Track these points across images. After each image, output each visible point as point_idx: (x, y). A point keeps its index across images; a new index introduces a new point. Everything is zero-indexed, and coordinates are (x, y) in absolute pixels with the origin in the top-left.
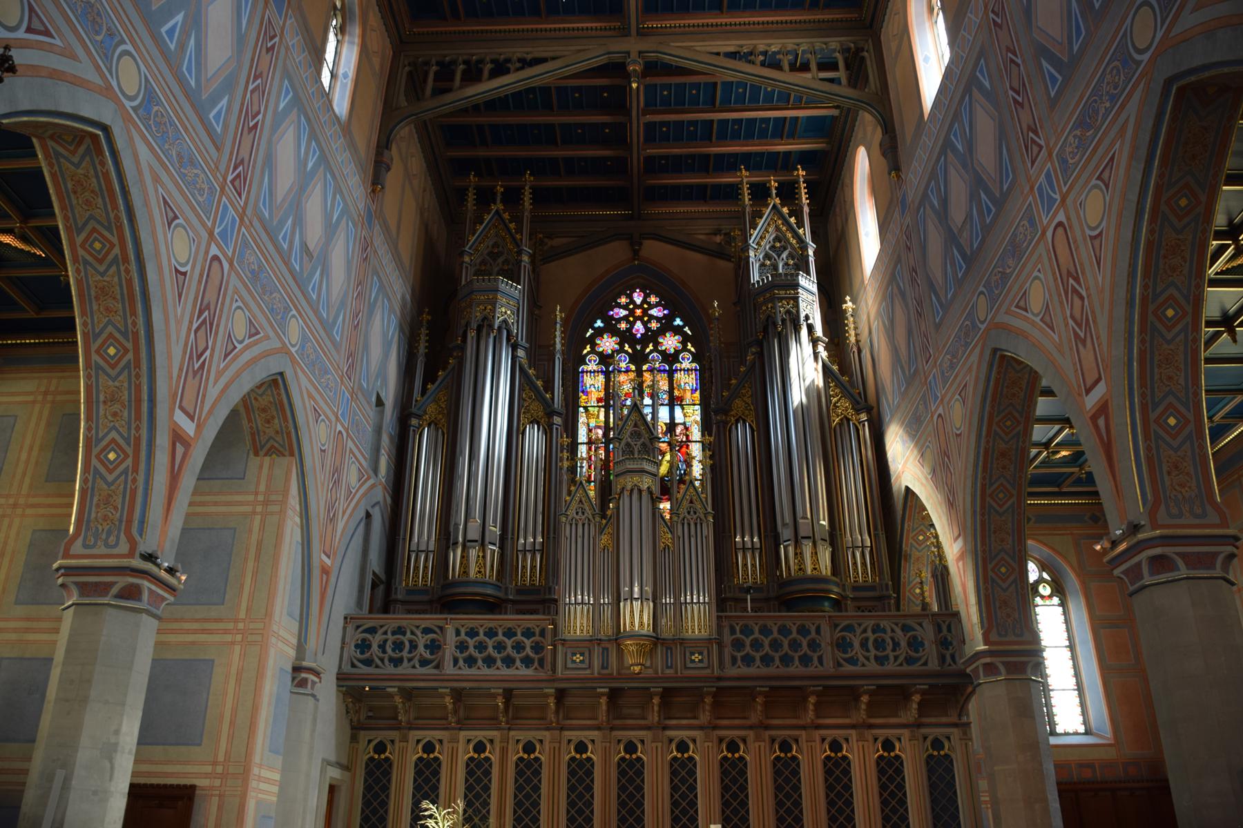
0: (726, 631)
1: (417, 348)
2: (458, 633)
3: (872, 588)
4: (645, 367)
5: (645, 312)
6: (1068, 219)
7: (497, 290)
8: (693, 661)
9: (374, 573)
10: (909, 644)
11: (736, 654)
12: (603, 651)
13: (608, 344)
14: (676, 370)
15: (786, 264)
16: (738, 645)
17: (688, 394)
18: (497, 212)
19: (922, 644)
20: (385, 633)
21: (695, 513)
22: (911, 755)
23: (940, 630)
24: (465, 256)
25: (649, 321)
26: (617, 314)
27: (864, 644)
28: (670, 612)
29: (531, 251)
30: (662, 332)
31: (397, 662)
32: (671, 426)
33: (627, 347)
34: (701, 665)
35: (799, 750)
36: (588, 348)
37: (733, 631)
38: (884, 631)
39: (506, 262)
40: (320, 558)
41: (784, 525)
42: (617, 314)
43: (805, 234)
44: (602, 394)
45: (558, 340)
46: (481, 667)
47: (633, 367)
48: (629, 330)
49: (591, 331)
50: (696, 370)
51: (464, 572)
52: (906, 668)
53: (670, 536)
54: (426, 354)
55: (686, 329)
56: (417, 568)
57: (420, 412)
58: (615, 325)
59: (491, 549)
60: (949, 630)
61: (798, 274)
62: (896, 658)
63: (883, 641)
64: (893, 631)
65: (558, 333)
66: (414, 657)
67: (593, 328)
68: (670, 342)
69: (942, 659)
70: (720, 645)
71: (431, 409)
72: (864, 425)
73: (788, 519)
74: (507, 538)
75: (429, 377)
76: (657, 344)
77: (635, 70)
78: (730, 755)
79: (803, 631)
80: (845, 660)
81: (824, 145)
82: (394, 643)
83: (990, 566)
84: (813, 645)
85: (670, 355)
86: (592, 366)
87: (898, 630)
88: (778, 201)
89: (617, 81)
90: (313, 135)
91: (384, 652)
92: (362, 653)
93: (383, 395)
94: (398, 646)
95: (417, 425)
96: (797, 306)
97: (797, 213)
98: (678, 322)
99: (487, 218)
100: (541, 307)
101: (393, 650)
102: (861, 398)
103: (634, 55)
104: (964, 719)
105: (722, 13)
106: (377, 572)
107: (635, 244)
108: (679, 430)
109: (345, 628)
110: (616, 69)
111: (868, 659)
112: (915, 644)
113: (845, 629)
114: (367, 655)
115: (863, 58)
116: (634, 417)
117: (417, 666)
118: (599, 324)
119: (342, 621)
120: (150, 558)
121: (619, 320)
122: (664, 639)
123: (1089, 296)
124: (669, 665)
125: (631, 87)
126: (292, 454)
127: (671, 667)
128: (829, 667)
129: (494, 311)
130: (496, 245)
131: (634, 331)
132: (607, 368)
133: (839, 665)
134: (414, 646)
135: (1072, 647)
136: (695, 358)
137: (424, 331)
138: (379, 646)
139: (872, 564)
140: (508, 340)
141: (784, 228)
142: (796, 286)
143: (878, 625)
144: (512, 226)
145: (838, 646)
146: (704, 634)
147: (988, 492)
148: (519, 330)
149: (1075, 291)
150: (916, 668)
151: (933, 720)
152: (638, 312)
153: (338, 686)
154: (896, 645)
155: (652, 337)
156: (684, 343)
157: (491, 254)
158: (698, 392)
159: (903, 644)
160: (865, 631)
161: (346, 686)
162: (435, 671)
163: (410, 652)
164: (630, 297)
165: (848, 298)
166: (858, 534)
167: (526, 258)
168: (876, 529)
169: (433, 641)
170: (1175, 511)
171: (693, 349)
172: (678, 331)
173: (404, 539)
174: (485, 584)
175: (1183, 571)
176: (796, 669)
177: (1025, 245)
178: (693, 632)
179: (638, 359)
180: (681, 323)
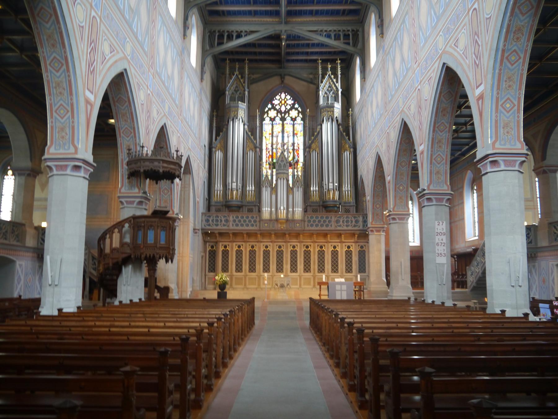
0: (306, 218)
2: (233, 217)
3: (350, 203)
6: (479, 7)
7: (238, 107)
13: (273, 113)
16: (309, 221)
17: (299, 132)
19: (359, 222)
22: (355, 250)
27: (343, 221)
28: (291, 213)
30: (291, 109)
31: (217, 225)
32: (293, 144)
33: (279, 115)
36: (266, 115)
37: (308, 217)
39: (240, 93)
40: (197, 199)
41: (325, 184)
44: (271, 132)
47: (281, 122)
48: (280, 109)
49: (267, 109)
56: (217, 195)
61: (334, 103)
62: (351, 225)
65: (258, 120)
68: (294, 113)
69: (364, 226)
71: (218, 146)
73: (327, 183)
75: (217, 135)
76: (289, 114)
77: (283, 38)
78: (306, 249)
80: (338, 226)
83: (374, 205)
84: (330, 221)
87: (353, 218)
88: (330, 73)
89: (277, 42)
90: (191, 81)
92: (207, 222)
94: (217, 221)
96: (333, 114)
97: (336, 77)
98: (296, 106)
99: (234, 77)
101: (216, 222)
103: (283, 32)
105: (313, 16)
107: (282, 77)
108: (296, 145)
110: (277, 37)
111: (344, 225)
112: (357, 221)
113: (338, 217)
115: (358, 35)
116: (282, 156)
119: (201, 214)
120: (177, 214)
123: (482, 45)
125: (282, 44)
126: (190, 174)
128: (333, 228)
129: (237, 114)
130: (237, 87)
133: (336, 227)
134: (221, 221)
136: (302, 119)
137: (215, 118)
138: (212, 221)
140: (242, 121)
142: (333, 107)
147: (376, 186)
148: (246, 120)
149: (476, 41)
151: (362, 241)
152: (283, 102)
155: (287, 112)
157: (235, 90)
160: (344, 218)
165: (350, 109)
166: (347, 187)
167: (246, 93)
172: (296, 109)
174: (238, 201)
175: (434, 203)
176: (324, 228)
177: (461, 15)
178: (297, 218)
179: (283, 119)
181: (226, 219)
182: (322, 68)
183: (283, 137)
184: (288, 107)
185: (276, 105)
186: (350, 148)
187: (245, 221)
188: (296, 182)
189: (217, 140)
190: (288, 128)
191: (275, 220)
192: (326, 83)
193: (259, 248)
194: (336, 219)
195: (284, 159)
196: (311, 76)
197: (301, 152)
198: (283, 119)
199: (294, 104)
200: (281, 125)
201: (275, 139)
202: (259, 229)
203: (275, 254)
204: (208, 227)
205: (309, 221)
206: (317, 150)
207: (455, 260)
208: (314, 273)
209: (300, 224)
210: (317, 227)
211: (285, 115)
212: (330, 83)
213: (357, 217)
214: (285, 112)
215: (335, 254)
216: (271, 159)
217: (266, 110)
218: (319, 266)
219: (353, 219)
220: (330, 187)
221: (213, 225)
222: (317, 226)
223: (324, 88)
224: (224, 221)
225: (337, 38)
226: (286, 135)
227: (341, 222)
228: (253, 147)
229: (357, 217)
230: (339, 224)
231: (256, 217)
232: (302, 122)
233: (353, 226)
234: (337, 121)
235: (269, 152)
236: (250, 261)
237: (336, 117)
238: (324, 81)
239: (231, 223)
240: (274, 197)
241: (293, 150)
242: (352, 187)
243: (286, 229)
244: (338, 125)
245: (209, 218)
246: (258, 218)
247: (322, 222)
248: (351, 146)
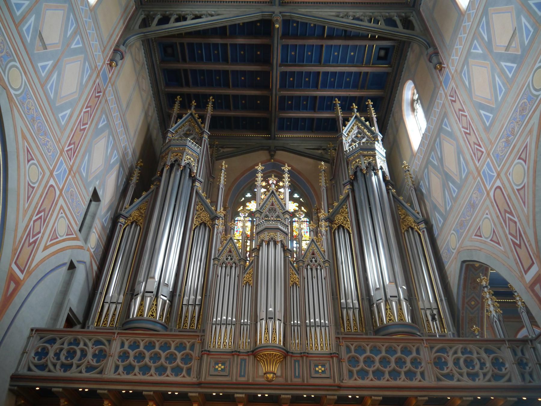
0: (343, 349)
8: (317, 372)
9: (71, 310)
10: (493, 364)
11: (351, 368)
12: (241, 363)
16: (353, 361)
18: (191, 114)
20: (63, 344)
21: (316, 261)
24: (169, 134)
27: (456, 362)
29: (209, 133)
34: (323, 375)
36: (241, 208)
43: (375, 130)
45: (222, 178)
46: (137, 374)
51: (140, 315)
52: (493, 383)
53: (297, 276)
54: (137, 183)
55: (301, 199)
57: (127, 215)
59: (163, 299)
62: (485, 375)
66: (83, 363)
70: (340, 361)
72: (423, 231)
74: (176, 295)
75: (136, 195)
81: (383, 93)
82: (68, 352)
84: (415, 362)
91: (58, 359)
93: (100, 193)
94: (71, 354)
95: (124, 223)
99: (185, 117)
100: (214, 178)
101: (66, 358)
102: (420, 216)
106: (75, 310)
109: (29, 338)
112: (497, 363)
114: (43, 361)
117: (84, 371)
119: (27, 333)
122: (292, 353)
124: (297, 375)
127: (299, 377)
128: (430, 381)
130: (189, 130)
133: (439, 379)
134: (84, 354)
141: (363, 128)
143: (465, 349)
145: (436, 364)
146: (326, 350)
150: (501, 383)
153: (10, 385)
154: (483, 365)
156: (299, 207)
159: (488, 364)
160: (455, 353)
161: (18, 386)
162: (98, 376)
163: (80, 360)
169: (101, 351)
171: (305, 211)
173: (101, 293)
180: (298, 197)
181: (101, 351)
187: (156, 357)
191: (248, 353)
192: (352, 128)
194: (433, 355)
195: (276, 206)
202: (195, 380)
204: (38, 372)
205: (353, 361)
209: (327, 366)
212: (358, 128)
219: (484, 355)
221: (55, 365)
222: (378, 374)
224: (94, 356)
227: (451, 364)
228: (207, 219)
230: (445, 371)
231: (192, 347)
239: (111, 363)
240: (247, 292)
243: (281, 380)
245: (48, 345)
247: (393, 365)
248: (418, 219)
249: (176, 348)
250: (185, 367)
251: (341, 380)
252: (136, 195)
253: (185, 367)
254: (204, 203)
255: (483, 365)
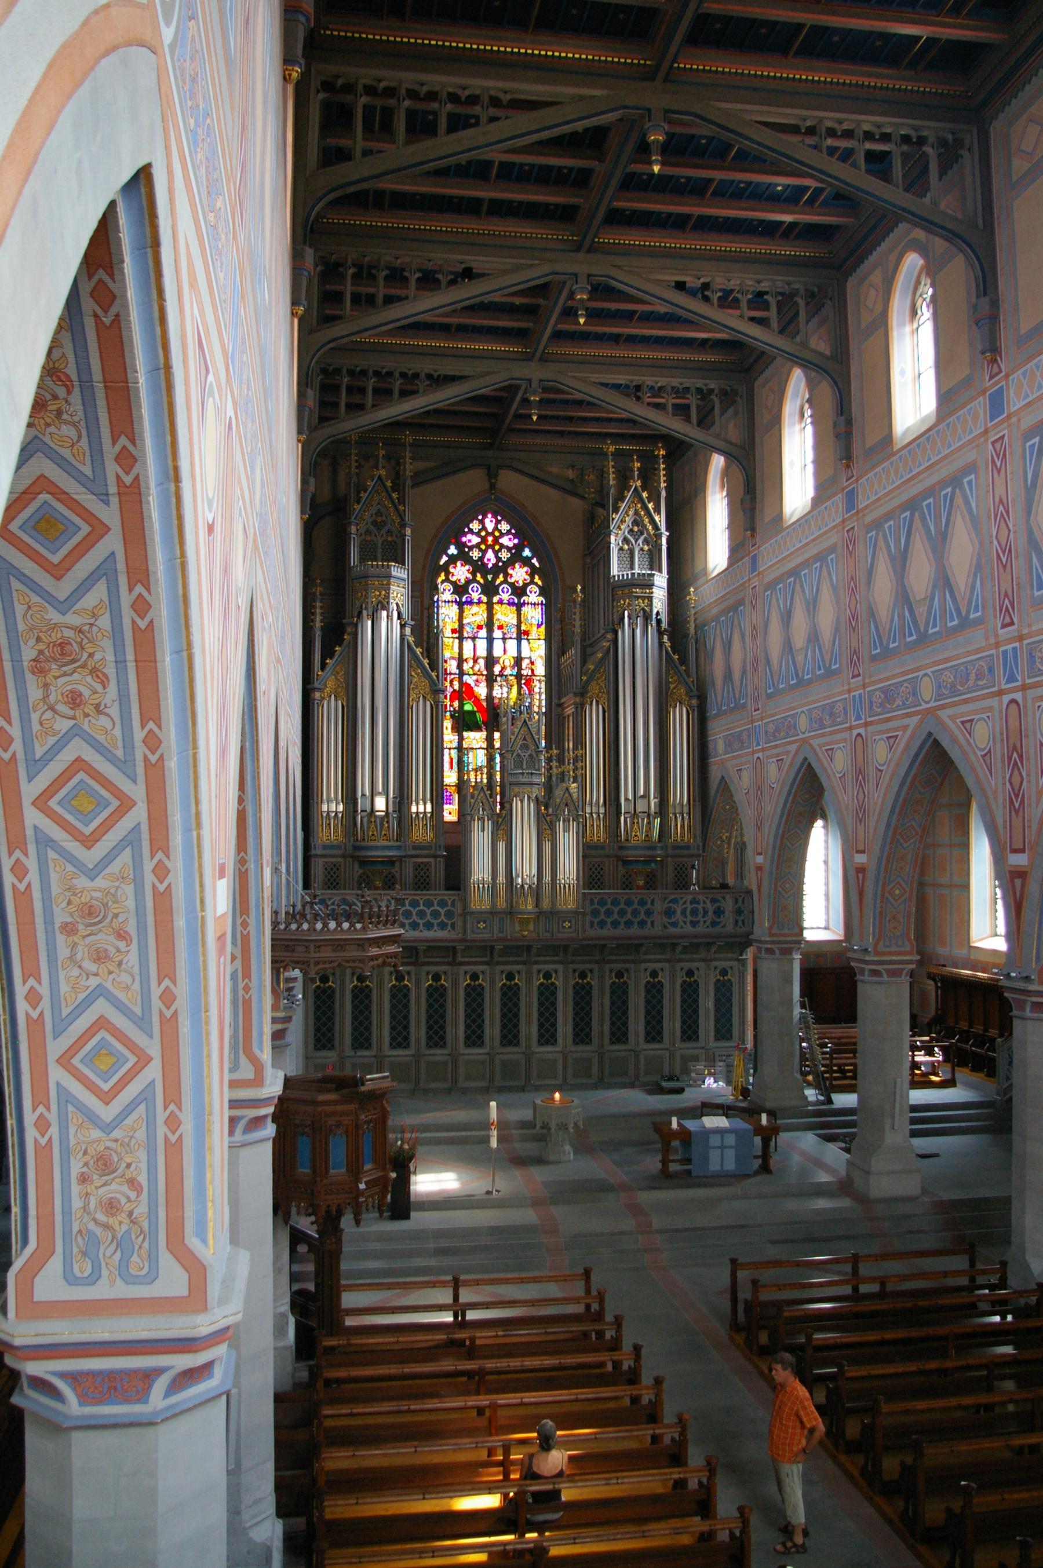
0: (588, 903)
1: (313, 621)
3: (688, 847)
4: (495, 599)
5: (496, 540)
7: (390, 576)
10: (715, 912)
13: (461, 572)
14: (524, 604)
15: (642, 549)
18: (380, 478)
19: (723, 912)
23: (737, 902)
25: (500, 550)
26: (470, 541)
27: (684, 912)
30: (511, 563)
32: (518, 661)
33: (479, 577)
35: (629, 978)
36: (443, 577)
37: (592, 902)
38: (698, 903)
42: (470, 541)
44: (456, 626)
47: (484, 599)
49: (445, 559)
50: (542, 604)
52: (710, 930)
53: (549, 832)
55: (534, 561)
58: (468, 553)
60: (743, 902)
63: (697, 910)
64: (704, 902)
67: (447, 555)
68: (519, 574)
71: (331, 683)
75: (328, 652)
76: (507, 575)
79: (642, 903)
84: (649, 913)
85: (519, 588)
86: (447, 596)
88: (639, 483)
96: (651, 605)
97: (655, 498)
98: (527, 553)
104: (744, 957)
107: (492, 475)
108: (525, 663)
111: (685, 923)
112: (719, 912)
113: (672, 901)
118: (453, 550)
121: (471, 548)
128: (657, 930)
129: (387, 596)
130: (379, 513)
131: (485, 560)
132: (461, 599)
135: (826, 862)
136: (543, 592)
139: (689, 826)
143: (694, 899)
144: (395, 495)
150: (717, 930)
152: (490, 539)
154: (706, 912)
155: (501, 568)
157: (374, 523)
158: (543, 627)
159: (710, 913)
160: (685, 903)
164: (482, 522)
168: (694, 800)
170: (887, 943)
171: (540, 583)
172: (526, 562)
176: (635, 931)
179: (490, 590)
182: (617, 472)
183: (490, 640)
184: (505, 555)
185: (471, 548)
186: (691, 697)
188: (562, 806)
189: (328, 669)
190: (505, 615)
192: (627, 513)
193: (455, 984)
196: (571, 474)
197: (539, 687)
198: (490, 590)
199: (519, 548)
200: (484, 607)
201: (468, 645)
203: (498, 995)
206: (604, 700)
207: (937, 988)
208: (602, 1045)
210: (615, 928)
211: (495, 578)
212: (636, 513)
213: (718, 901)
214: (497, 570)
215: (654, 991)
216: (456, 704)
217: (442, 562)
218: (613, 1024)
220: (639, 810)
222: (615, 924)
223: (622, 527)
225: (682, 411)
226: (497, 634)
228: (428, 690)
229: (718, 901)
230: (673, 920)
232: (541, 599)
233: (708, 923)
234: (659, 622)
235: (452, 681)
236: (430, 1017)
237: (658, 613)
238: (623, 506)
240: (502, 846)
241: (519, 677)
242: (694, 805)
244: (660, 633)
246: (459, 905)
249: (439, 905)
250: (449, 922)
251: (584, 931)
252: (328, 652)
253: (449, 922)
254: (420, 664)
255: (706, 912)
